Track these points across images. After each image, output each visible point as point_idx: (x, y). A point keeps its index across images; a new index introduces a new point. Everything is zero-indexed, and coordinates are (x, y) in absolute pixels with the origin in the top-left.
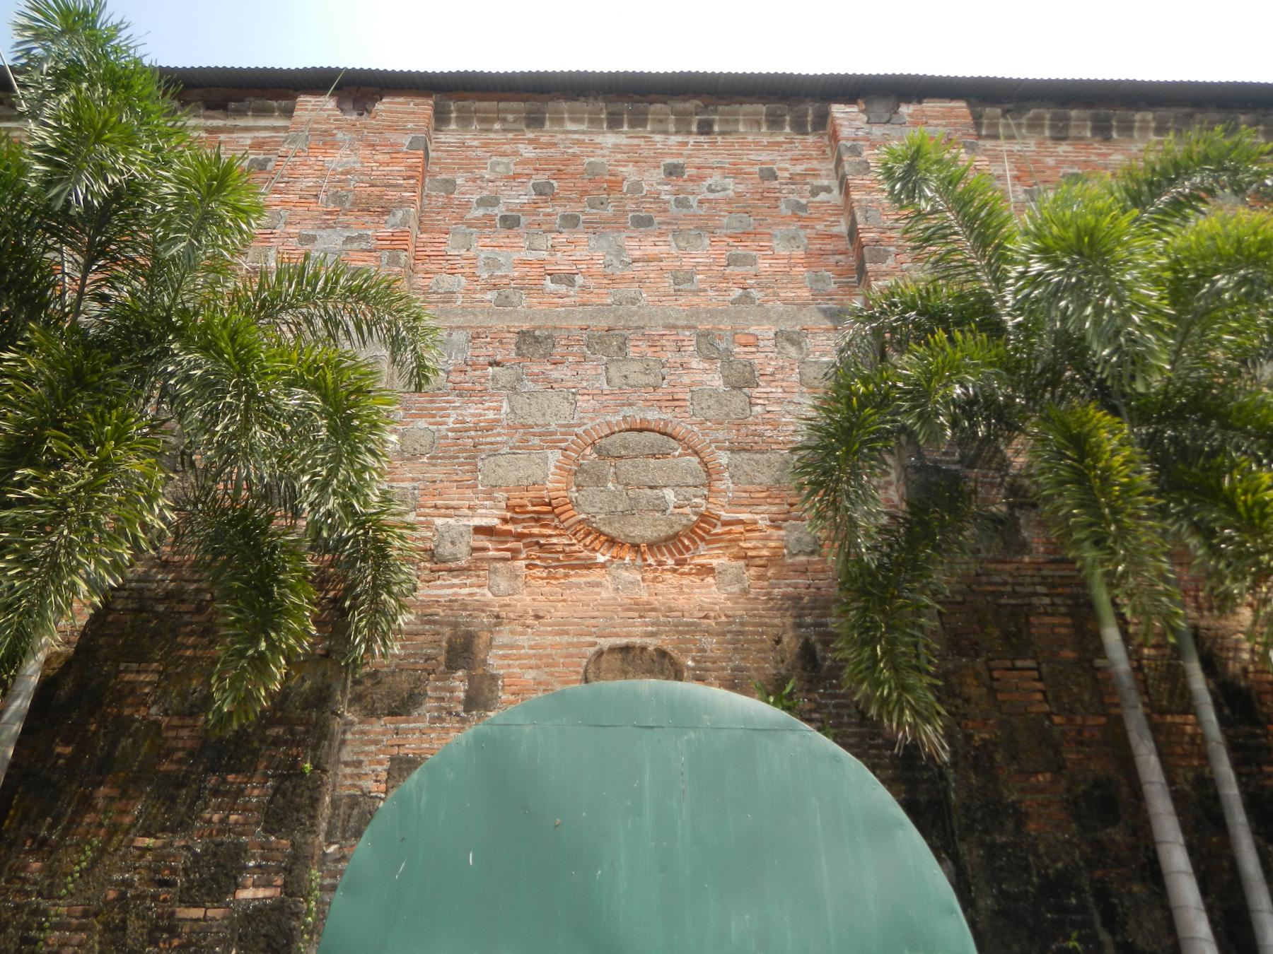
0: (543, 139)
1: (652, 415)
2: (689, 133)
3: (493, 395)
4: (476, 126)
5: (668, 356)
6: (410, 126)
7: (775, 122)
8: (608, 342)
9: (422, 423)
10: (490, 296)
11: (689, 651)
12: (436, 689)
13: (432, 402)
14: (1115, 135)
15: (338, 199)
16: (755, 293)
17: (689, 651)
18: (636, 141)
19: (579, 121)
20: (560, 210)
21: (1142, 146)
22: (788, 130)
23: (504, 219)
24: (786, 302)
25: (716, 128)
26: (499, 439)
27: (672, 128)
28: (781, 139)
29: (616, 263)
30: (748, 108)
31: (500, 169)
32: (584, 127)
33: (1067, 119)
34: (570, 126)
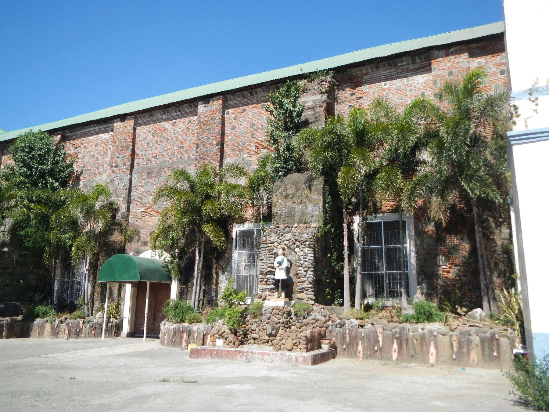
7: (191, 107)
9: (135, 193)
15: (121, 147)
16: (183, 156)
34: (158, 115)
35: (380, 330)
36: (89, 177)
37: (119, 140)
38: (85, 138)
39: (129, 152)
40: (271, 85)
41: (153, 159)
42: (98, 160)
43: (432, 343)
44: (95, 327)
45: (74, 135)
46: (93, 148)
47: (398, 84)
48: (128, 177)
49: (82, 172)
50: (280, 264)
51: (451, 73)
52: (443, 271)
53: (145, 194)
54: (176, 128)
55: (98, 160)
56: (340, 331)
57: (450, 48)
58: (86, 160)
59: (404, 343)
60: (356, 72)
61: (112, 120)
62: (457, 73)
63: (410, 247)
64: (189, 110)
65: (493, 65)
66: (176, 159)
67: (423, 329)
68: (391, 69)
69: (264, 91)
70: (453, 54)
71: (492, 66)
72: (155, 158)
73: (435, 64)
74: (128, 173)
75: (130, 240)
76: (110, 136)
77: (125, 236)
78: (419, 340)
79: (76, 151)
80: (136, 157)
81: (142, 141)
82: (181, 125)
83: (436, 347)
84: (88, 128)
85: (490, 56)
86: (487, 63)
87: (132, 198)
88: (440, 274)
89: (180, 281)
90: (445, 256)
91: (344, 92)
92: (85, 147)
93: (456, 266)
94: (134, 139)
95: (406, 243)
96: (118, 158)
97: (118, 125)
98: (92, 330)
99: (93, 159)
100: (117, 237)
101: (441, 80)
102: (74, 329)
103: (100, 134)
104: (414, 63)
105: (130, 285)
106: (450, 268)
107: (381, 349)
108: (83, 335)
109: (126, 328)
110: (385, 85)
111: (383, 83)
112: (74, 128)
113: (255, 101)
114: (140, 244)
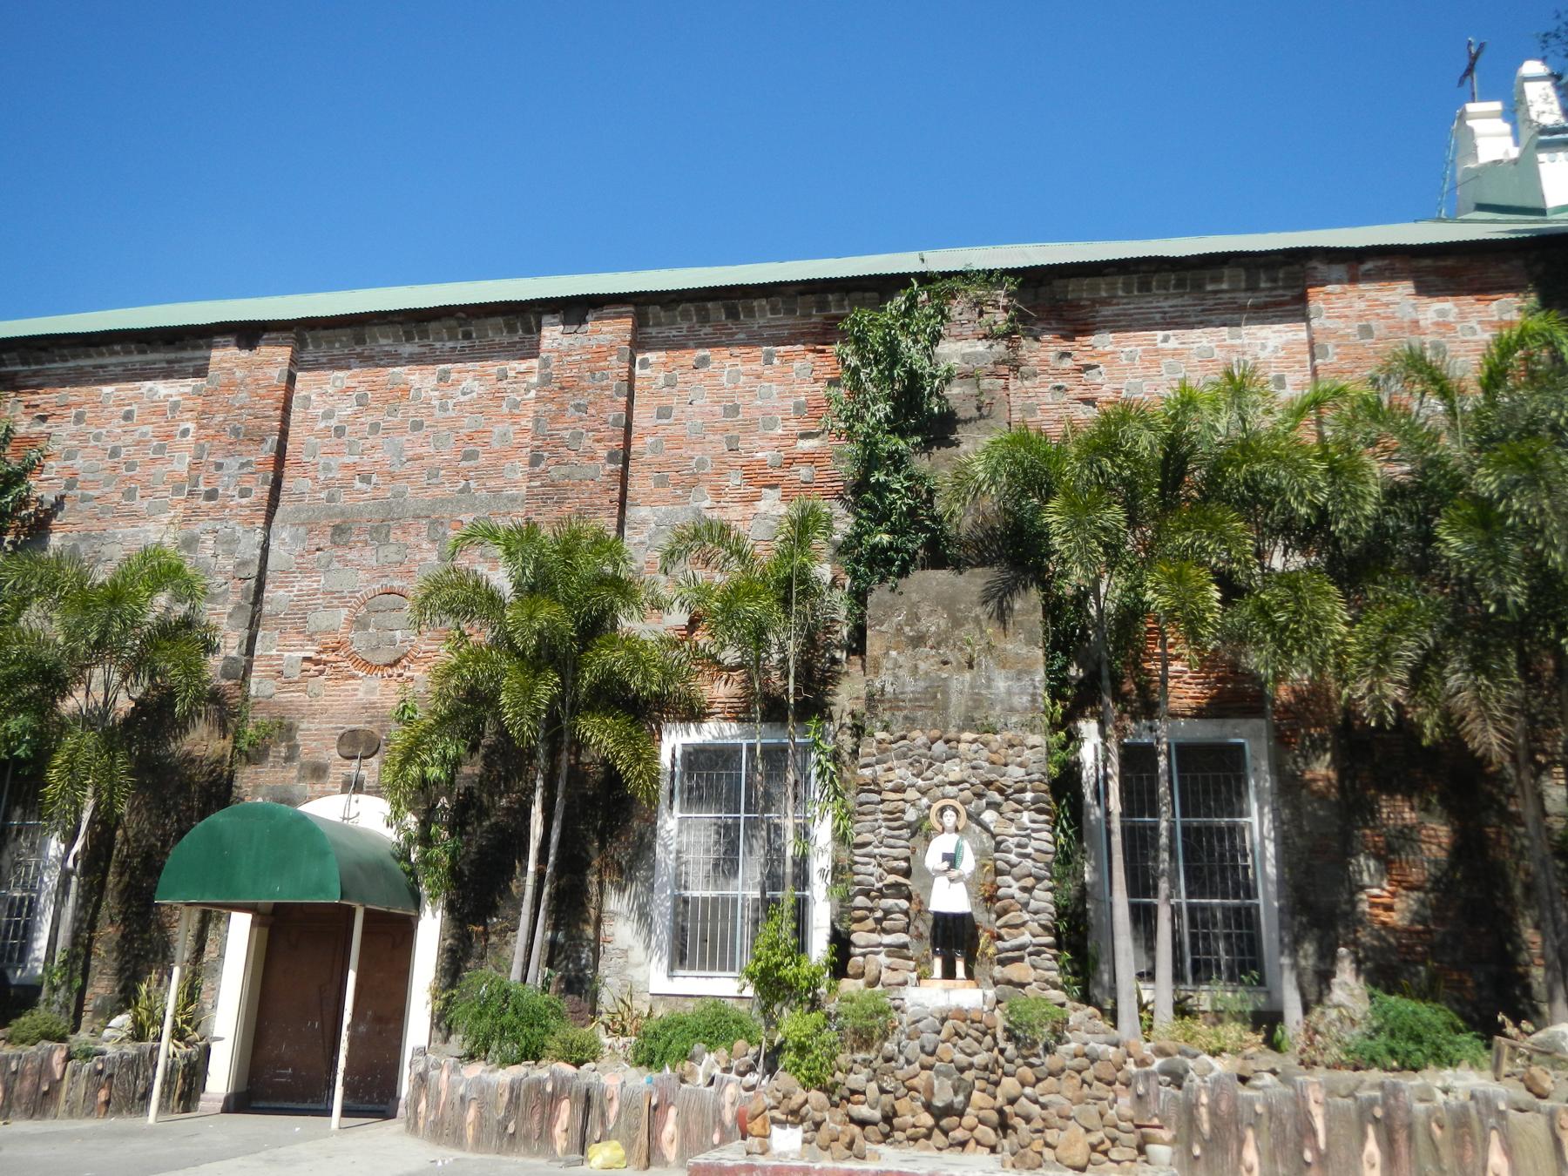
1: (397, 584)
4: (324, 346)
5: (412, 540)
7: (512, 330)
9: (281, 592)
15: (236, 431)
16: (473, 484)
19: (387, 337)
21: (762, 322)
24: (489, 490)
27: (446, 337)
31: (338, 383)
33: (707, 310)
34: (382, 341)
35: (1314, 1095)
36: (88, 523)
37: (229, 408)
38: (84, 390)
39: (267, 450)
40: (802, 294)
41: (358, 485)
42: (131, 466)
43: (1494, 1137)
44: (111, 1076)
45: (35, 374)
46: (116, 426)
47: (1205, 342)
48: (259, 537)
49: (59, 503)
50: (952, 860)
51: (1366, 331)
52: (1373, 905)
53: (320, 600)
54: (450, 391)
55: (131, 466)
56: (1175, 1097)
57: (1362, 262)
58: (79, 463)
59: (1401, 1137)
60: (1077, 290)
61: (200, 337)
62: (1385, 332)
63: (1258, 824)
64: (505, 338)
65: (1480, 322)
66: (448, 490)
67: (1446, 1091)
68: (1182, 296)
69: (774, 310)
70: (1369, 277)
71: (1478, 327)
72: (366, 479)
73: (1318, 299)
74: (260, 523)
75: (256, 755)
78: (1449, 1129)
79: (43, 427)
80: (288, 472)
81: (314, 419)
82: (469, 382)
83: (1508, 1150)
84: (101, 355)
85: (1470, 299)
86: (1463, 316)
87: (267, 608)
88: (1364, 913)
89: (451, 908)
90: (1378, 857)
91: (1037, 345)
92: (79, 418)
93: (1411, 888)
94: (286, 409)
95: (1249, 815)
96: (219, 466)
97: (224, 356)
98: (100, 1087)
99: (110, 463)
100: (202, 742)
101: (1338, 346)
102: (27, 1084)
103: (148, 379)
104: (1252, 288)
105: (248, 917)
106: (1393, 894)
107: (1323, 1159)
108: (62, 1106)
109: (220, 1079)
110: (1166, 339)
111: (1160, 334)
112: (44, 349)
113: (742, 336)
114: (294, 773)
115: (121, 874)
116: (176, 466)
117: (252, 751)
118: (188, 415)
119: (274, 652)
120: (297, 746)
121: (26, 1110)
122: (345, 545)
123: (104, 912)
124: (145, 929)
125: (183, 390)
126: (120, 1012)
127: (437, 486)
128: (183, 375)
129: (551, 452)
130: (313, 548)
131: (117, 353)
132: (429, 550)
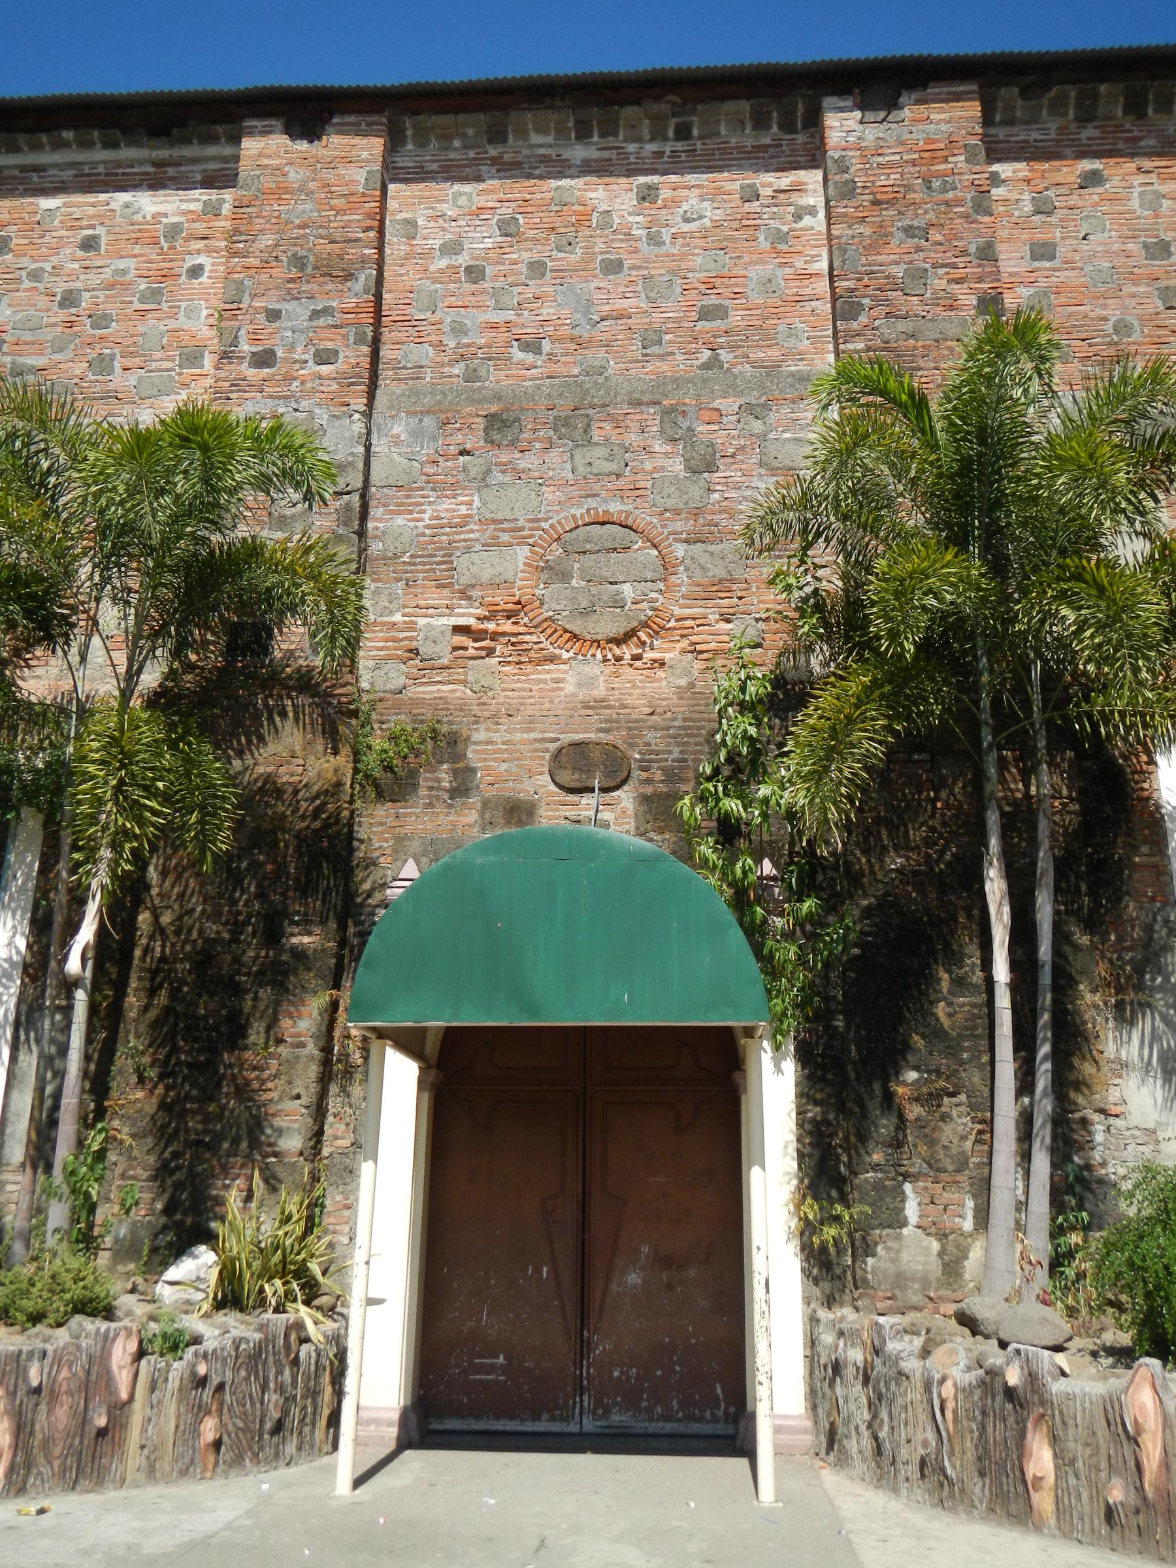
0: (507, 157)
1: (615, 507)
2: (666, 139)
3: (465, 488)
4: (434, 144)
5: (633, 439)
6: (364, 155)
7: (761, 123)
8: (573, 422)
9: (400, 520)
10: (457, 370)
11: (637, 745)
12: (427, 779)
13: (408, 497)
14: (1150, 112)
15: (299, 262)
16: (724, 355)
17: (637, 745)
18: (606, 154)
20: (526, 255)
22: (775, 129)
23: (469, 270)
24: (755, 365)
25: (695, 132)
26: (472, 536)
27: (646, 134)
28: (767, 141)
29: (583, 321)
30: (731, 106)
31: (462, 201)
32: (550, 139)
33: (1095, 96)
34: (536, 139)
37: (281, 225)
41: (518, 355)
42: (101, 320)
44: (221, 1387)
46: (70, 259)
48: (358, 427)
55: (101, 320)
64: (748, 138)
66: (680, 365)
72: (531, 345)
74: (359, 403)
75: (393, 784)
76: (196, 207)
77: (356, 755)
82: (691, 202)
84: (37, 147)
87: (375, 547)
89: (804, 1055)
96: (274, 315)
97: (264, 149)
98: (202, 1411)
102: (62, 1415)
103: (123, 189)
108: (134, 1458)
113: (1152, 142)
114: (472, 817)
115: (152, 992)
116: (182, 322)
117: (385, 779)
118: (200, 245)
119: (398, 618)
120: (473, 770)
121: (64, 1469)
122: (513, 443)
123: (123, 1062)
124: (209, 1094)
125: (184, 207)
126: (179, 1250)
127: (662, 357)
128: (184, 184)
129: (873, 298)
130: (453, 450)
131: (66, 145)
132: (667, 455)
